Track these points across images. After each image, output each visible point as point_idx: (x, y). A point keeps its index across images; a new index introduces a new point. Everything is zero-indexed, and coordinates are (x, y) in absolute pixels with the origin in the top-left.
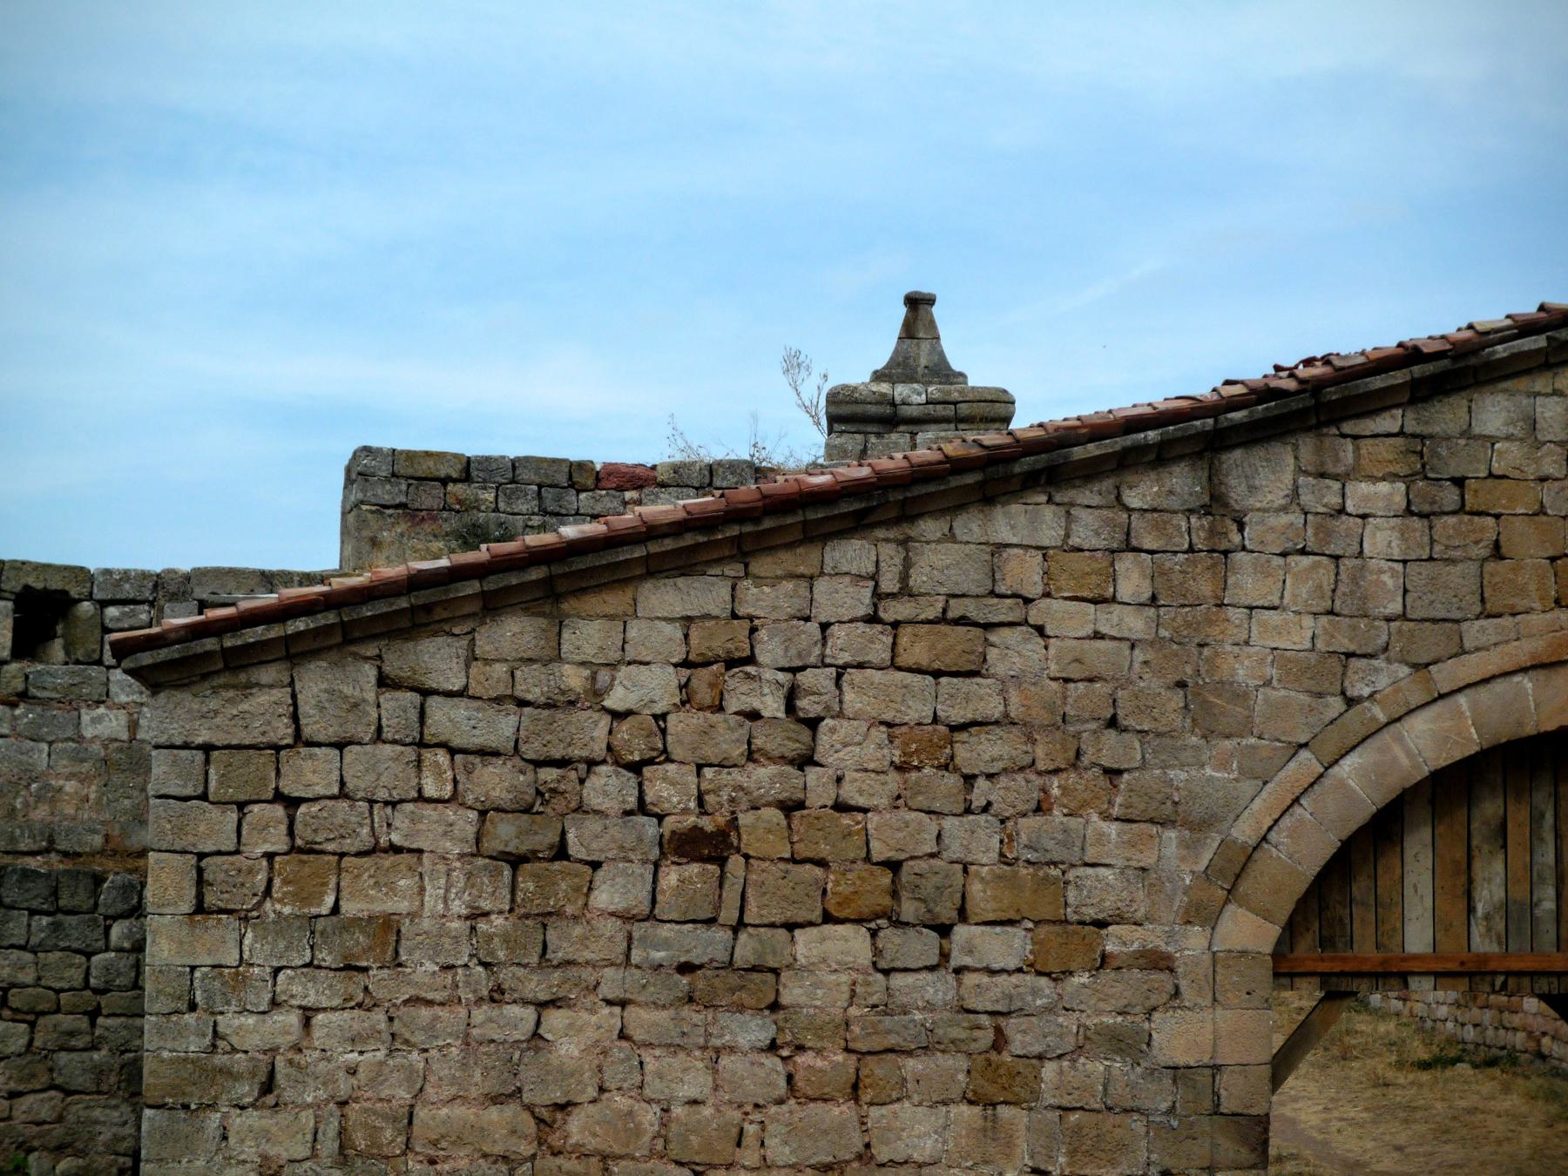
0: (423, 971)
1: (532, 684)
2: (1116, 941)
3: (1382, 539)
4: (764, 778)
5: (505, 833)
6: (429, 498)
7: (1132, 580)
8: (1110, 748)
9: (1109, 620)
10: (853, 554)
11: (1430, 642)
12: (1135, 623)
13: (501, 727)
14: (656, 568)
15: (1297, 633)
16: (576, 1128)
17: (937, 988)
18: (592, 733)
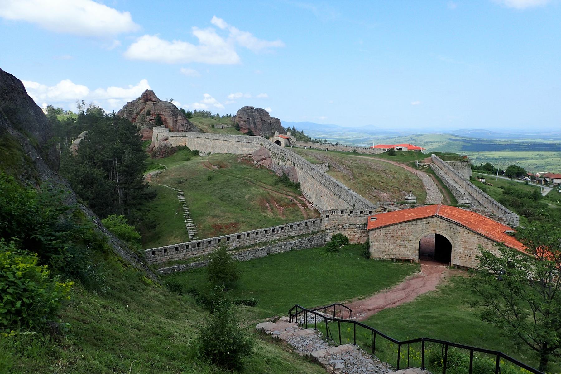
0: (381, 242)
1: (385, 230)
2: (411, 241)
3: (425, 225)
4: (395, 234)
5: (384, 236)
6: (382, 205)
7: (413, 226)
8: (411, 233)
9: (411, 228)
10: (400, 225)
11: (427, 229)
12: (413, 228)
13: (384, 232)
14: (391, 226)
15: (421, 229)
16: (387, 248)
17: (403, 243)
18: (388, 232)
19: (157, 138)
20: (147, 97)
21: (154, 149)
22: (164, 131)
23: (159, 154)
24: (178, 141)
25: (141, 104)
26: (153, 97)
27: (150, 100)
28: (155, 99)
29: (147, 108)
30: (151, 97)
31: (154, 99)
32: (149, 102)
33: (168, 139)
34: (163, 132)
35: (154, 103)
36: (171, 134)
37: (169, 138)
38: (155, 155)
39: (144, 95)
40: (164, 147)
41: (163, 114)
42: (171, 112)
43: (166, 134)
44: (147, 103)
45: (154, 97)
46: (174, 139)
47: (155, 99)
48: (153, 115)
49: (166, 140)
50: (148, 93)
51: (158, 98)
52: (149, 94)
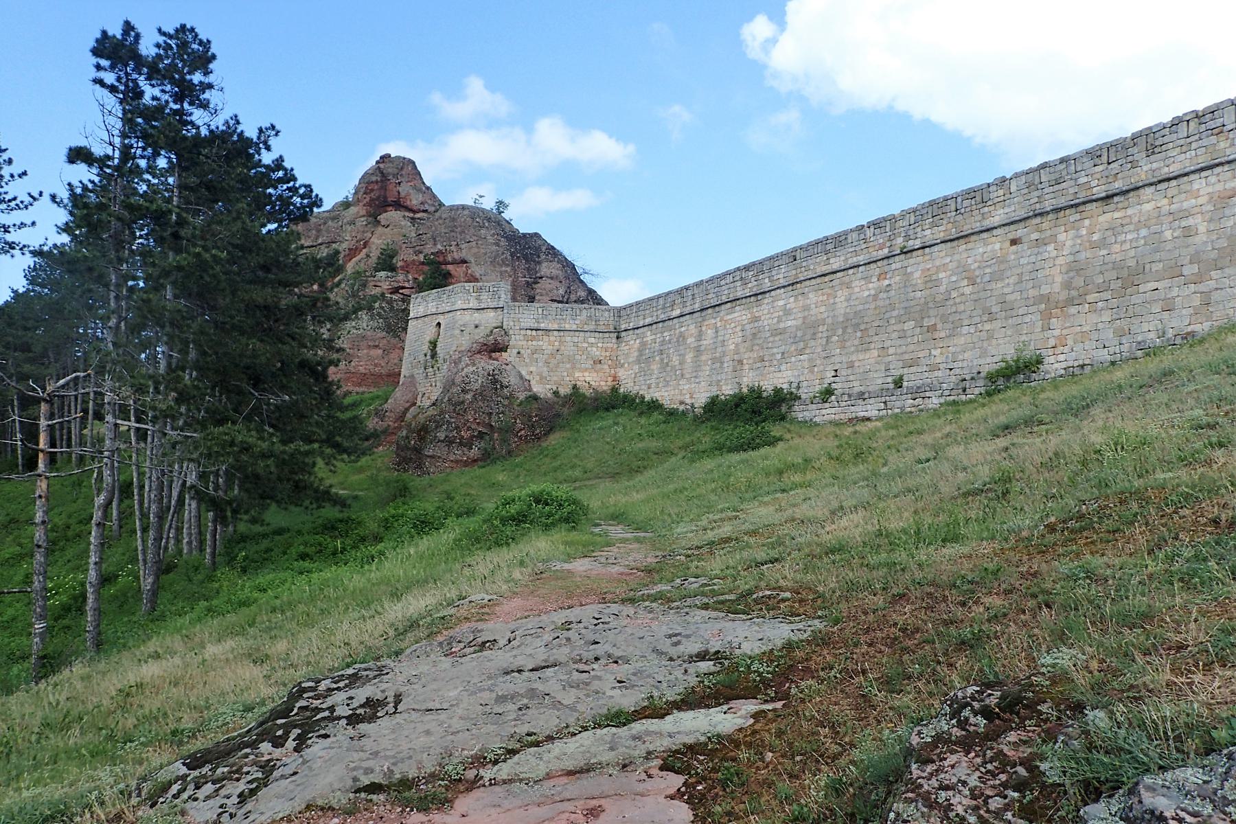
19: (434, 344)
20: (384, 188)
21: (409, 416)
22: (484, 296)
23: (449, 442)
24: (571, 360)
25: (352, 223)
26: (414, 187)
27: (399, 205)
28: (420, 197)
29: (378, 241)
30: (404, 189)
31: (415, 200)
32: (392, 215)
33: (504, 349)
34: (473, 304)
35: (418, 215)
36: (528, 315)
37: (516, 341)
38: (418, 451)
39: (370, 183)
40: (480, 395)
41: (464, 254)
42: (503, 242)
43: (492, 314)
44: (382, 218)
45: (419, 190)
46: (545, 344)
47: (420, 197)
48: (406, 268)
49: (494, 348)
50: (389, 168)
51: (434, 196)
52: (395, 176)
